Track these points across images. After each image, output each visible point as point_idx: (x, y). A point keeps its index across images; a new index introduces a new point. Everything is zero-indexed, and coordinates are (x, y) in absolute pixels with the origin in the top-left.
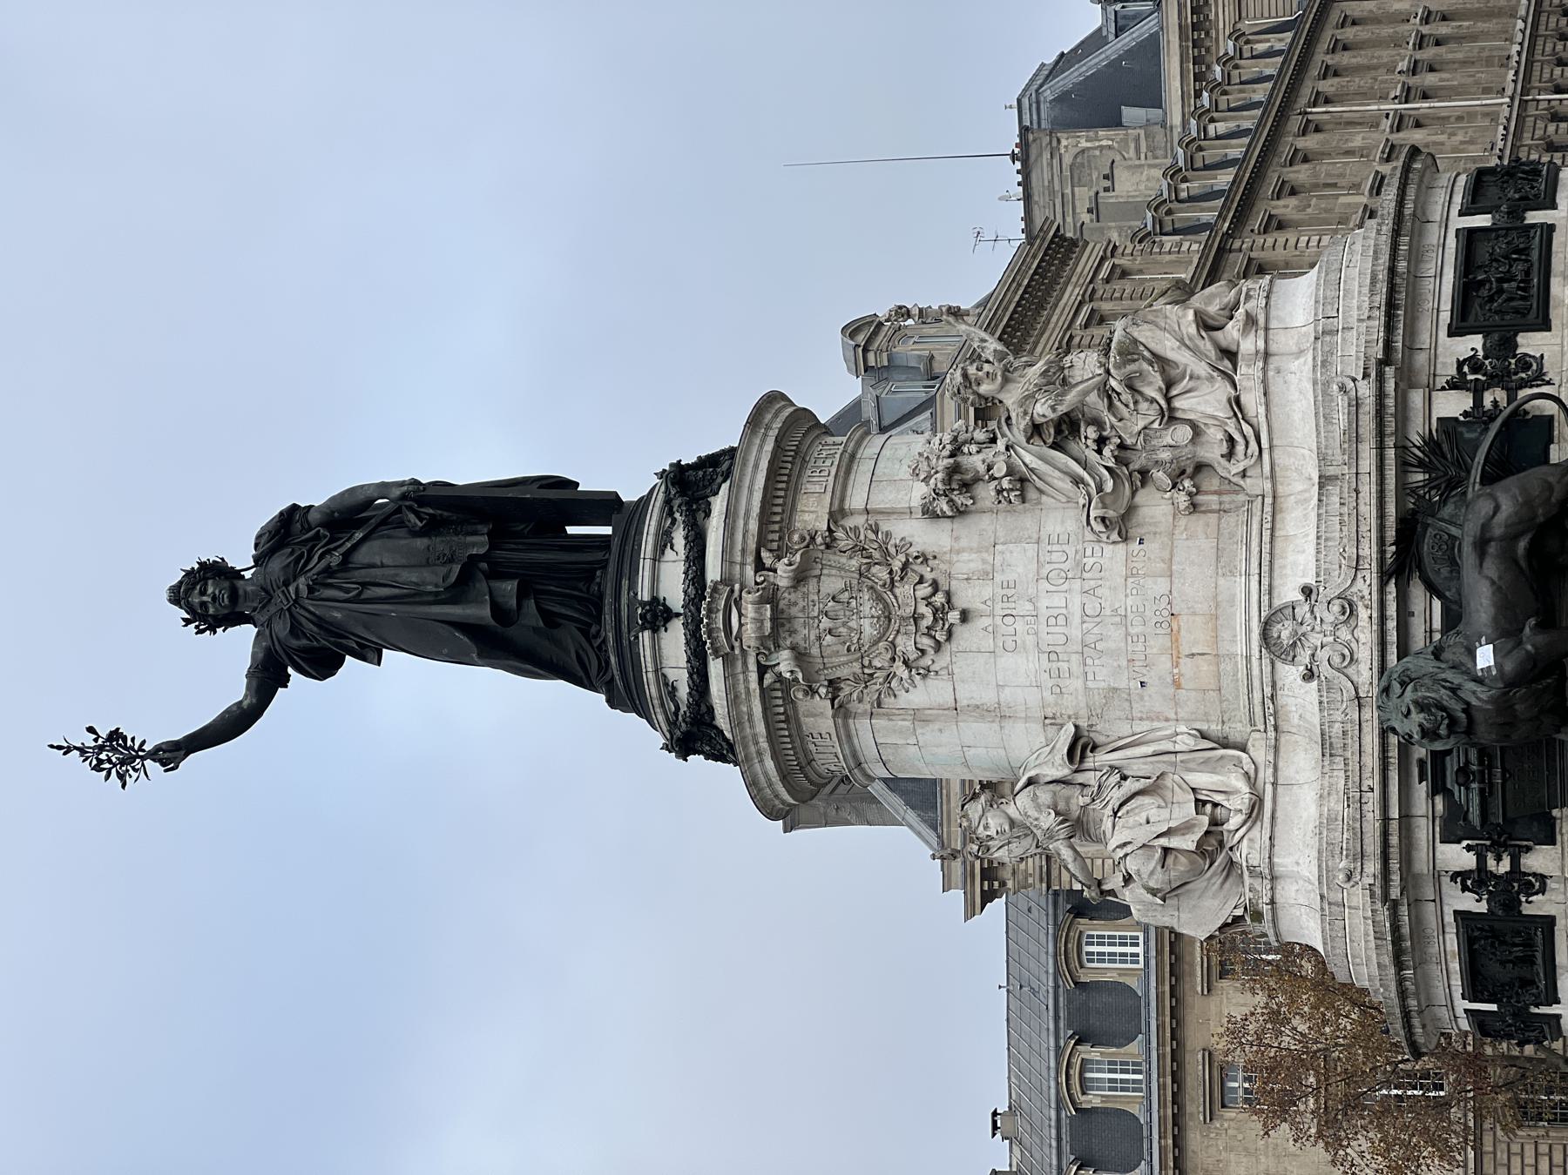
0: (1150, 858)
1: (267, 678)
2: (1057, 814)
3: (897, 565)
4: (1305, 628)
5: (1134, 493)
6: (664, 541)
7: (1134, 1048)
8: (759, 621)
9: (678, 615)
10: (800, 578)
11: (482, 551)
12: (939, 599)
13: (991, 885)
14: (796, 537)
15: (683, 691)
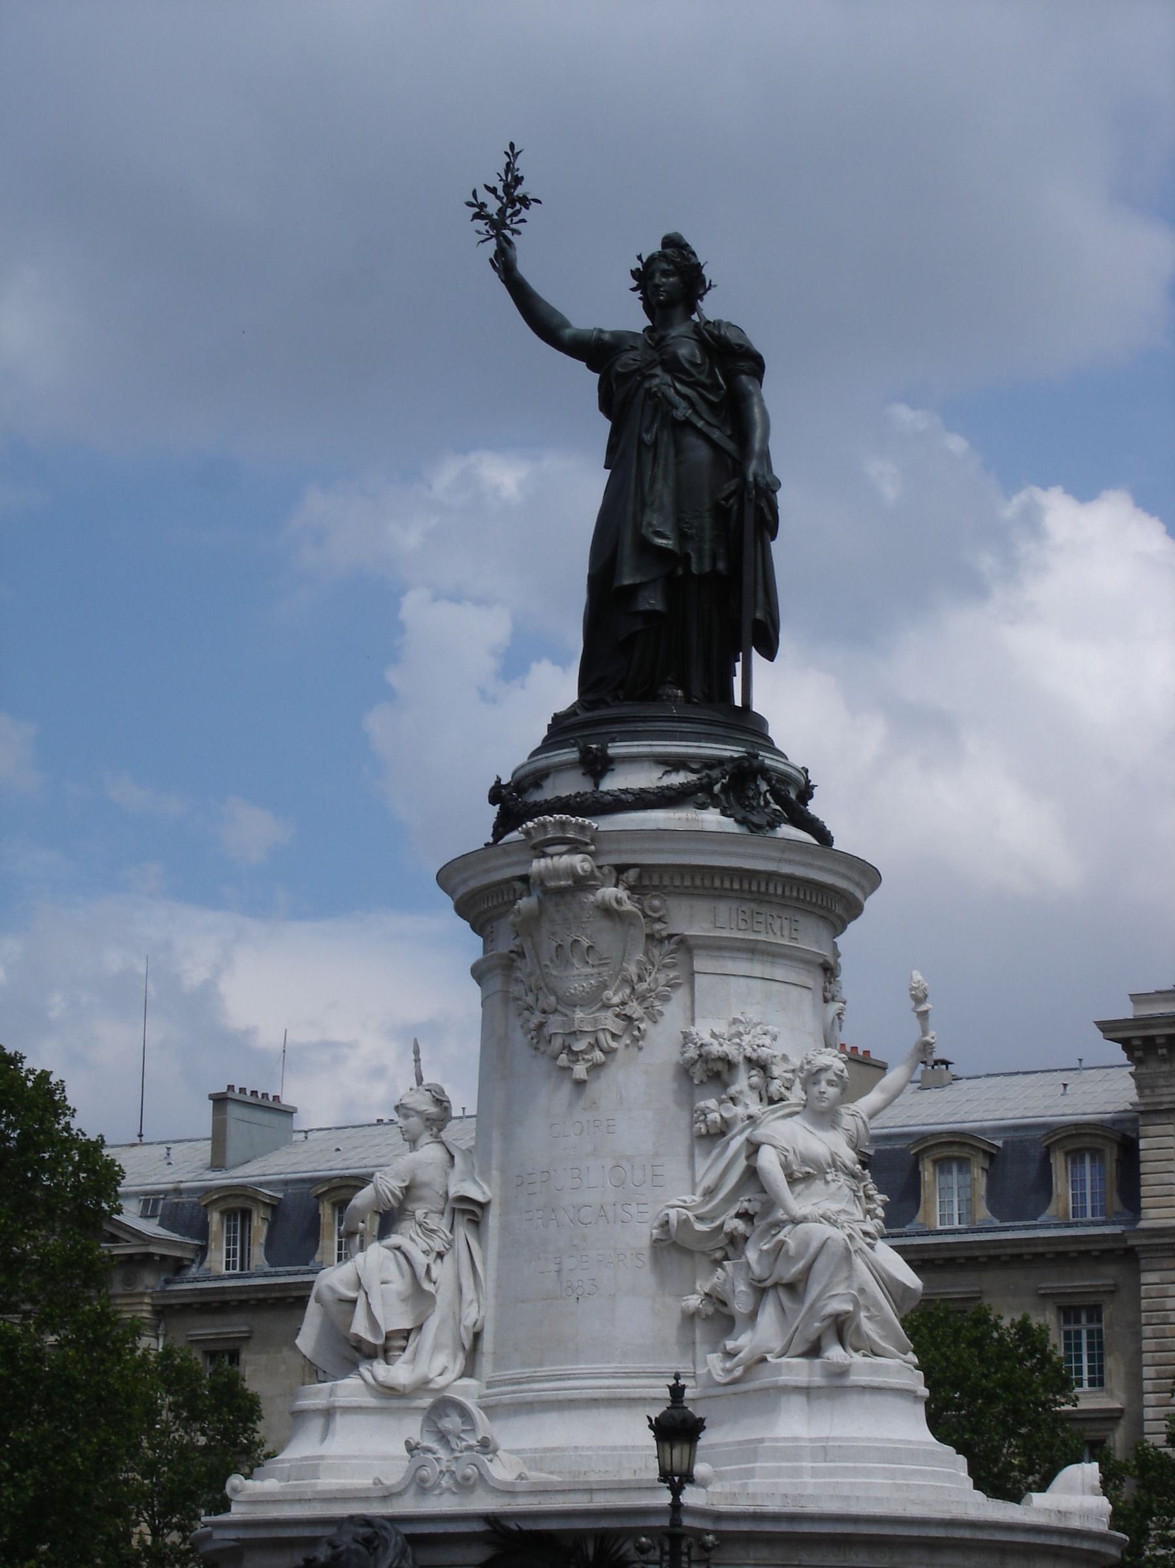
0: (347, 1285)
1: (595, 351)
2: (407, 1188)
3: (635, 1009)
4: (454, 1442)
5: (703, 1253)
6: (675, 764)
7: (983, 1213)
8: (556, 874)
9: (597, 785)
10: (607, 911)
11: (694, 569)
12: (598, 1055)
13: (1137, 1048)
14: (656, 903)
15: (537, 796)
